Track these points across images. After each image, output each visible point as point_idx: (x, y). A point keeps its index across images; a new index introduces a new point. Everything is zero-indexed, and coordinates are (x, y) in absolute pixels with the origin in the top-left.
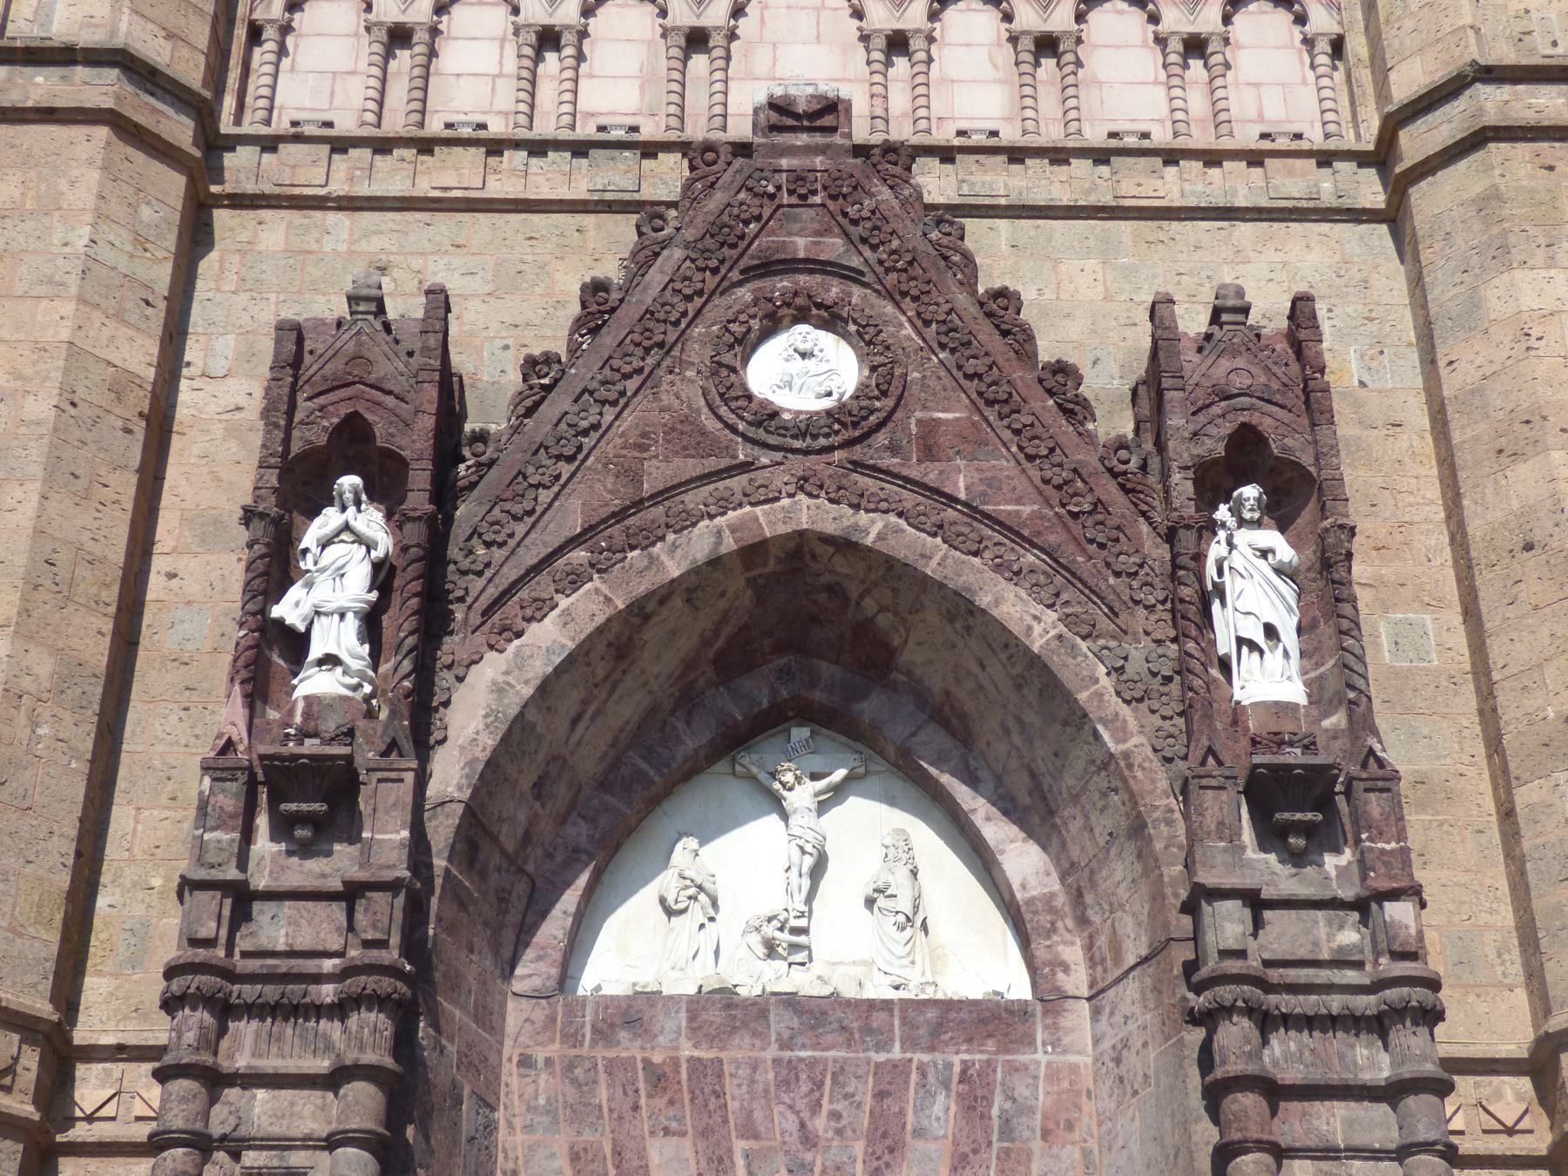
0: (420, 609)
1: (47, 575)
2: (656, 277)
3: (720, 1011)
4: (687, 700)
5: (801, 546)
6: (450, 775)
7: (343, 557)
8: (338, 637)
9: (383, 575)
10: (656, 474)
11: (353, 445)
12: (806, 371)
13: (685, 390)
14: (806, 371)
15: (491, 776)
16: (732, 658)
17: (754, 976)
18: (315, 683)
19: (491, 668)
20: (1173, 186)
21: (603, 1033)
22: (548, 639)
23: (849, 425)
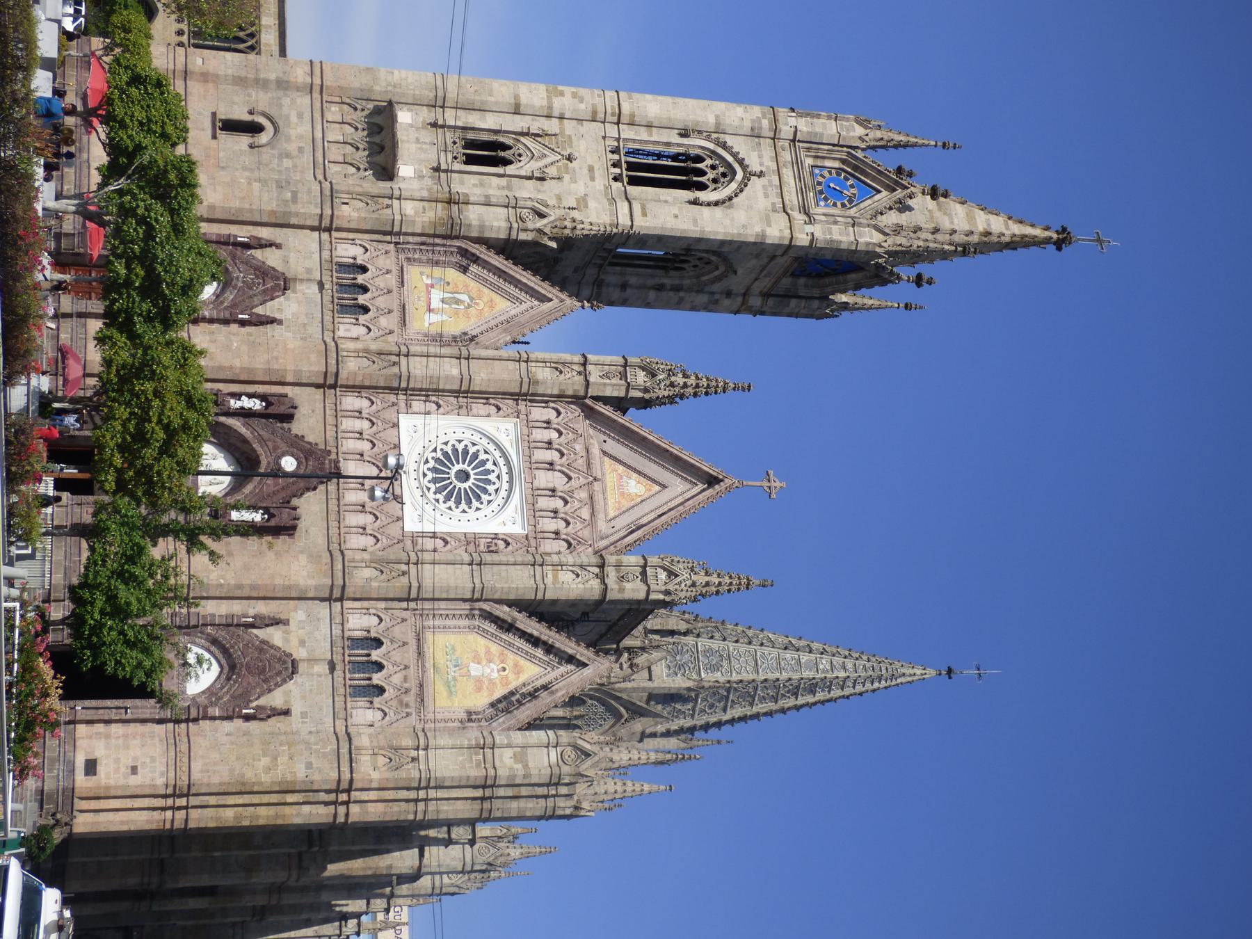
0: (245, 414)
1: (251, 371)
4: (243, 454)
5: (259, 462)
6: (222, 419)
7: (256, 404)
10: (270, 444)
11: (269, 404)
12: (289, 464)
13: (284, 447)
15: (223, 425)
16: (248, 459)
18: (232, 402)
20: (334, 524)
22: (243, 430)
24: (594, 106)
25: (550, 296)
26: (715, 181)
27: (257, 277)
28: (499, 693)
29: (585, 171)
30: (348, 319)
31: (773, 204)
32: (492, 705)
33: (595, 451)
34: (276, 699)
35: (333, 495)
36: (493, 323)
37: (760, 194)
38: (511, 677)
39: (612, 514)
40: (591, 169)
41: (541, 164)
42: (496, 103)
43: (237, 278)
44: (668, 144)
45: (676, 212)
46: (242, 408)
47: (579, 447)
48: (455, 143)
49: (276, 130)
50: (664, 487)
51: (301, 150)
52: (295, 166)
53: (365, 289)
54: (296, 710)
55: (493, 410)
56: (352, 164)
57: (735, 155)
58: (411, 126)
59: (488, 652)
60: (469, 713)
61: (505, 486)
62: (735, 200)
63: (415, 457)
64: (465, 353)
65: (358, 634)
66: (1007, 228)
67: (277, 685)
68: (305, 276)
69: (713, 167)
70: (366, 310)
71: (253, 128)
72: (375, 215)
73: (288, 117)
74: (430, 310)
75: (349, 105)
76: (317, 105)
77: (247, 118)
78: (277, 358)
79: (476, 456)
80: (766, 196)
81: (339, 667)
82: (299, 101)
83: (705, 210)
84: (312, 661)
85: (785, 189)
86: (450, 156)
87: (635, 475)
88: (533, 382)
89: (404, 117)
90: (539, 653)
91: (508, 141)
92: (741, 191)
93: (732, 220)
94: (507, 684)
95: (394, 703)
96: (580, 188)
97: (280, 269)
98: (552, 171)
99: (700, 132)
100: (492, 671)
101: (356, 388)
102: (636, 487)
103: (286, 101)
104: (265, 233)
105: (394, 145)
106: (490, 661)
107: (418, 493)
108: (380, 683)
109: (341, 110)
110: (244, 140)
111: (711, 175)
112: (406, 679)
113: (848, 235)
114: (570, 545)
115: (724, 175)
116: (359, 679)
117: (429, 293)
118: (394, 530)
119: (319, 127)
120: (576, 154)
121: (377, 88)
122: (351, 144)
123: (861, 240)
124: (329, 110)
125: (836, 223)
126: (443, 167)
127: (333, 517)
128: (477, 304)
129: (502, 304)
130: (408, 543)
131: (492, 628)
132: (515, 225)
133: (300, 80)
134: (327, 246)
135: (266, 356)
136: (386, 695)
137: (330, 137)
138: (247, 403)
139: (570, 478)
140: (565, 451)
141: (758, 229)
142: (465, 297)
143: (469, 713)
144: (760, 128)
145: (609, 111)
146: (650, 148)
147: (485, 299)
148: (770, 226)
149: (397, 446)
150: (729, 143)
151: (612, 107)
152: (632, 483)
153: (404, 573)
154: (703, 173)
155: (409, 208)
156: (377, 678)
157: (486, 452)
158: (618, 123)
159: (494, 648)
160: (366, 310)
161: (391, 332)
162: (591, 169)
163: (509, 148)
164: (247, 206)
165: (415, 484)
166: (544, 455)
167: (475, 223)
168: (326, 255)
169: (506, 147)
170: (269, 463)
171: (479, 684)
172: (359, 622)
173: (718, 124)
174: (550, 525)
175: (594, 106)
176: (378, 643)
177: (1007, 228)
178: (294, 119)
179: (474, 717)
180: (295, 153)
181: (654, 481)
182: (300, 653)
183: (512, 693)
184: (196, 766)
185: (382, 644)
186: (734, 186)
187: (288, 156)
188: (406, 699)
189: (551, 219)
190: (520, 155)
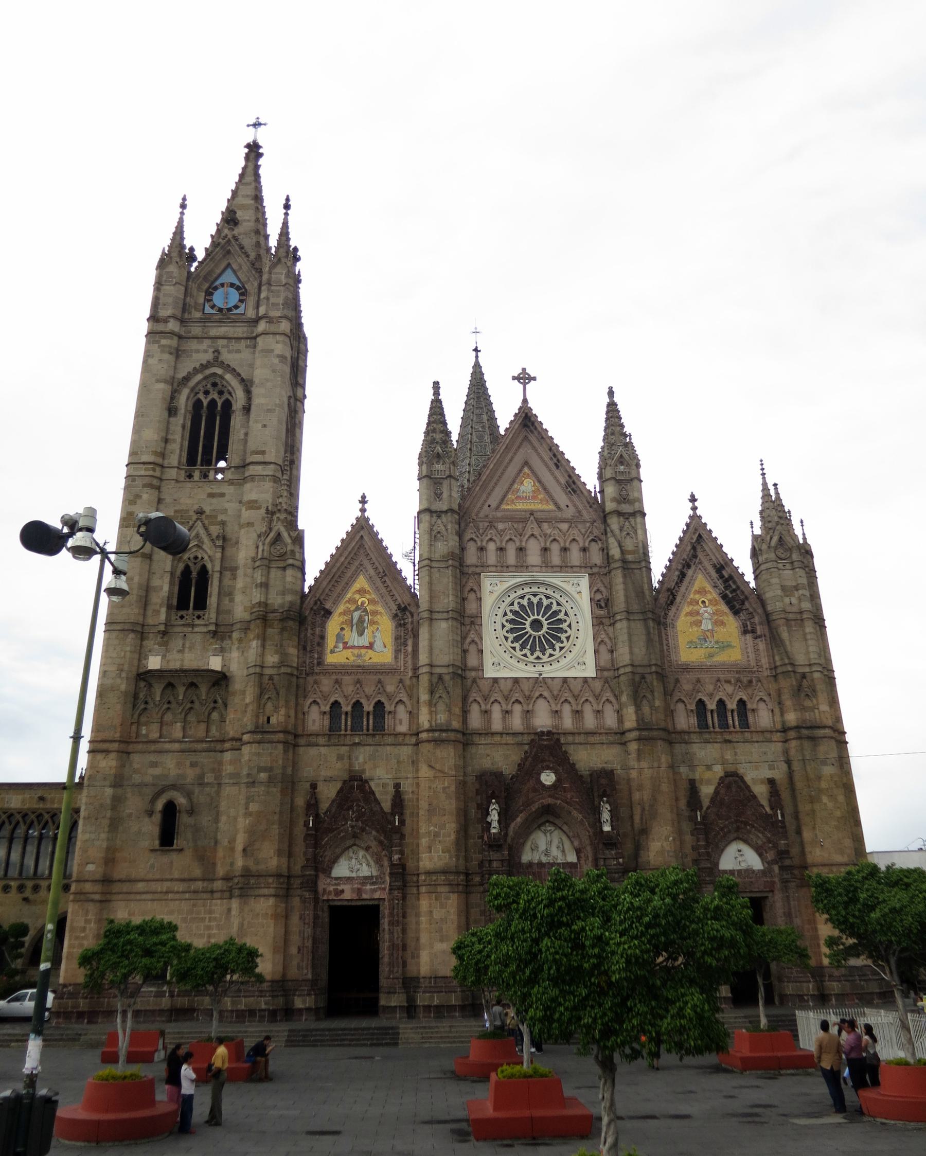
2: (528, 763)
3: (541, 865)
5: (549, 805)
8: (495, 824)
9: (499, 814)
12: (548, 778)
13: (531, 783)
14: (548, 778)
17: (544, 860)
18: (493, 831)
19: (513, 825)
20: (597, 739)
21: (527, 868)
23: (554, 786)
24: (145, 486)
25: (358, 538)
26: (221, 393)
27: (351, 807)
28: (724, 607)
29: (214, 501)
30: (388, 720)
31: (247, 347)
32: (736, 612)
33: (499, 514)
34: (761, 791)
35: (570, 738)
36: (383, 590)
37: (237, 356)
38: (709, 597)
39: (551, 507)
40: (211, 495)
41: (206, 540)
42: (140, 575)
43: (352, 827)
44: (184, 427)
45: (260, 425)
46: (499, 822)
47: (501, 526)
48: (182, 617)
49: (174, 787)
50: (526, 463)
51: (193, 765)
52: (213, 770)
53: (357, 705)
54: (769, 774)
55: (472, 596)
56: (210, 714)
57: (196, 371)
58: (164, 657)
59: (690, 614)
60: (745, 632)
61: (542, 590)
62: (244, 375)
63: (521, 665)
64: (425, 615)
65: (694, 720)
66: (250, 184)
67: (750, 791)
68: (346, 761)
69: (207, 393)
70: (379, 705)
71: (170, 810)
72: (282, 692)
73: (155, 777)
74: (371, 646)
75: (140, 715)
76: (140, 746)
77: (157, 818)
78: (444, 788)
79: (515, 613)
80: (238, 351)
81: (728, 737)
82: (136, 766)
83: (256, 401)
84: (724, 763)
85: (231, 335)
86: (197, 622)
87: (516, 486)
88: (452, 555)
89: (154, 663)
90: (690, 573)
91: (181, 566)
92: (234, 370)
93: (267, 380)
94: (716, 600)
95: (750, 691)
96: (232, 507)
97: (339, 785)
98: (215, 530)
99: (172, 398)
100: (707, 612)
101: (465, 712)
102: (527, 486)
103: (137, 779)
104: (300, 801)
105: (197, 672)
106: (698, 613)
107: (556, 665)
108: (715, 703)
109: (146, 724)
110: (184, 820)
111: (214, 395)
112: (728, 682)
113: (279, 291)
114: (593, 540)
115: (215, 385)
116: (733, 720)
117: (353, 647)
118: (598, 685)
119: (167, 746)
120: (196, 507)
121: (123, 687)
122: (186, 715)
123: (284, 281)
124: (146, 735)
125: (268, 299)
126: (212, 628)
127: (591, 739)
128: (363, 603)
129: (361, 582)
130: (606, 674)
131: (673, 609)
132: (291, 561)
133: (114, 763)
134: (313, 740)
135: (443, 796)
136: (745, 698)
137: (178, 734)
138: (494, 816)
139: (533, 535)
140: (508, 537)
141: (276, 361)
142: (356, 615)
143: (745, 632)
144: (170, 347)
145: (151, 473)
146: (186, 443)
147: (357, 596)
148: (272, 351)
149: (516, 681)
150: (184, 374)
151: (146, 470)
152: (522, 488)
153: (643, 677)
154: (213, 403)
155: (272, 659)
156: (732, 705)
157: (512, 604)
158: (162, 466)
159: (687, 609)
160: (379, 705)
161: (401, 681)
162: (211, 495)
163: (187, 567)
164: (276, 817)
165: (547, 668)
166: (511, 557)
167: (289, 598)
168: (321, 740)
169: (187, 571)
170: (550, 796)
171: (719, 623)
172: (684, 720)
173: (165, 381)
174: (575, 556)
175: (145, 486)
176: (701, 703)
177: (250, 184)
178: (157, 771)
179: (749, 628)
180: (198, 770)
181: (521, 471)
182: (719, 771)
183: (724, 597)
184: (839, 858)
185: (700, 700)
186: (228, 377)
187: (201, 776)
188: (745, 680)
189: (282, 529)
190: (196, 558)
